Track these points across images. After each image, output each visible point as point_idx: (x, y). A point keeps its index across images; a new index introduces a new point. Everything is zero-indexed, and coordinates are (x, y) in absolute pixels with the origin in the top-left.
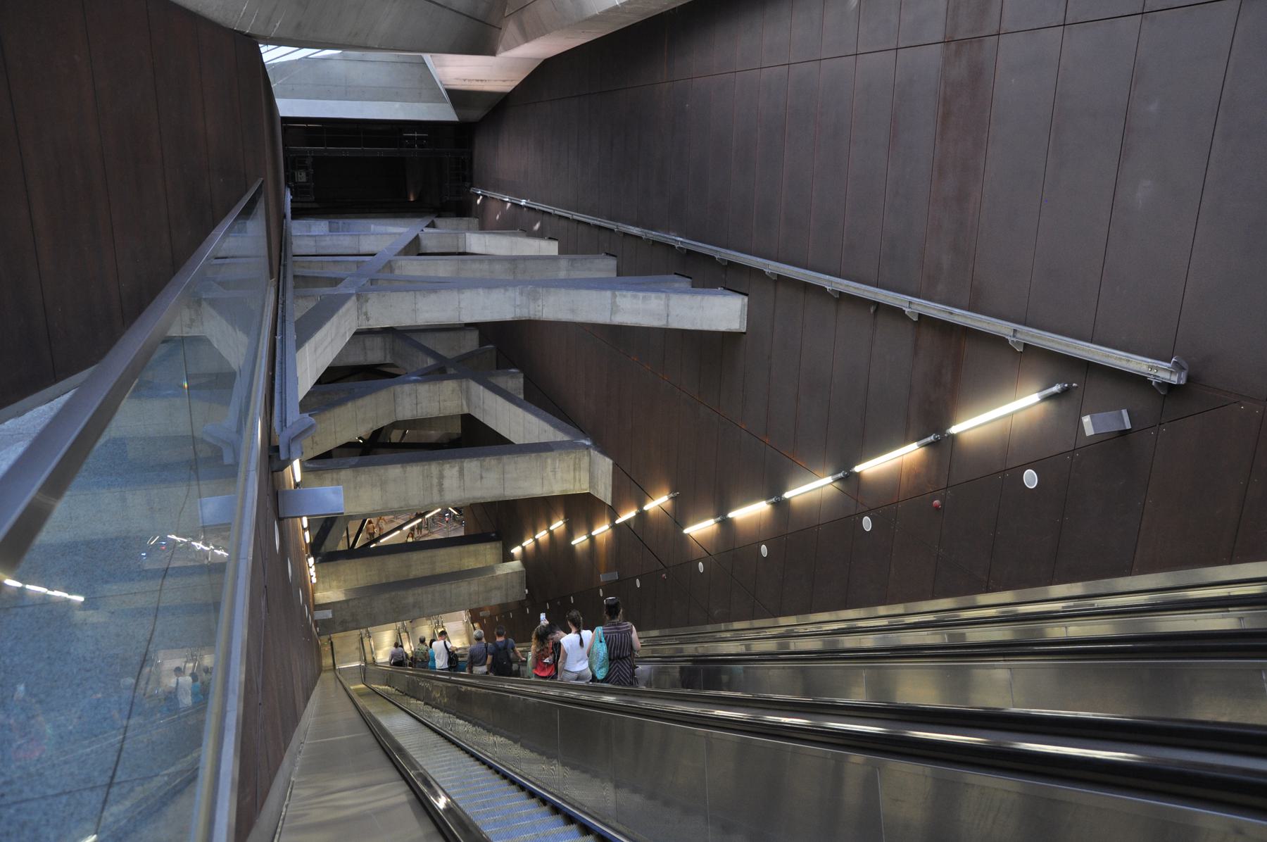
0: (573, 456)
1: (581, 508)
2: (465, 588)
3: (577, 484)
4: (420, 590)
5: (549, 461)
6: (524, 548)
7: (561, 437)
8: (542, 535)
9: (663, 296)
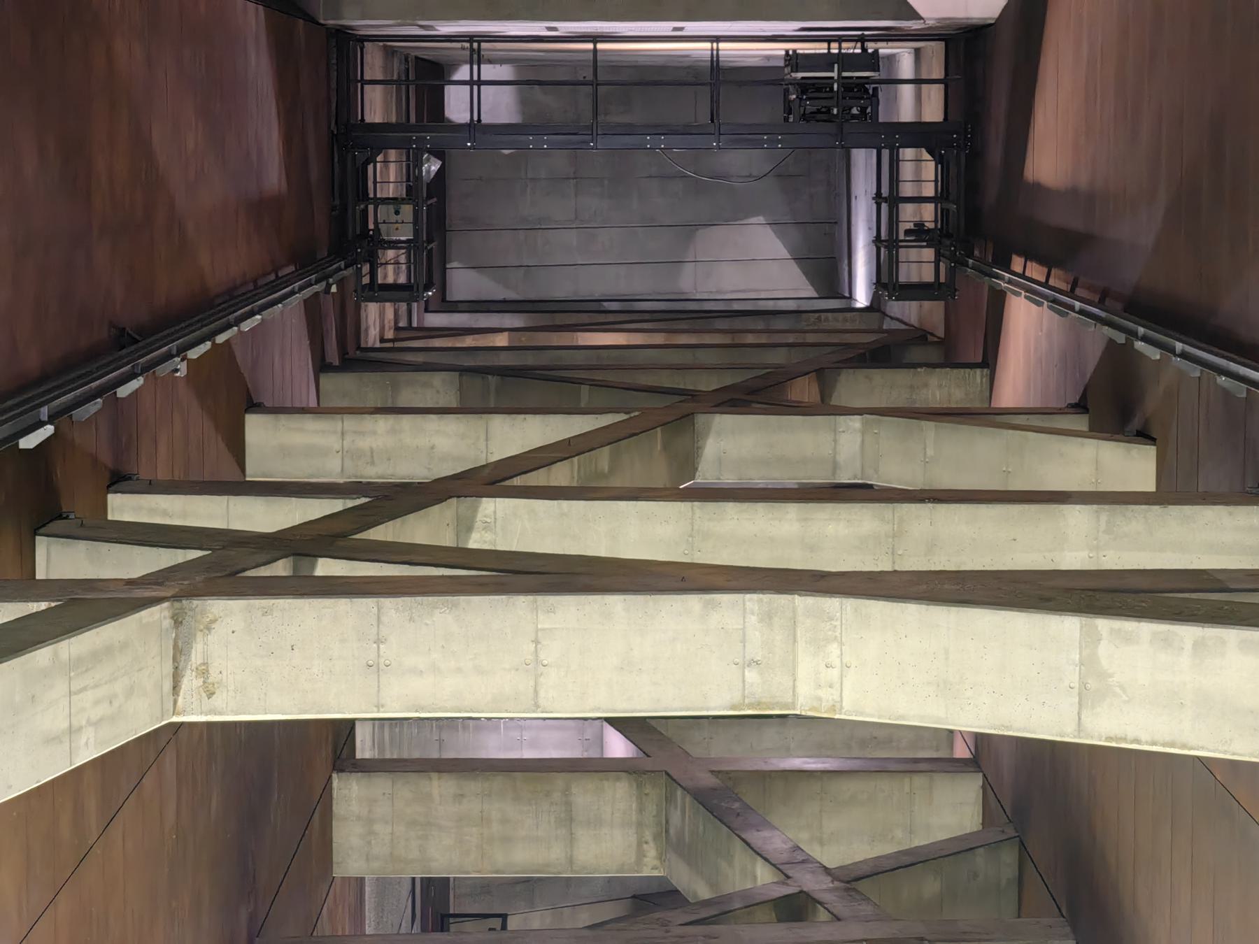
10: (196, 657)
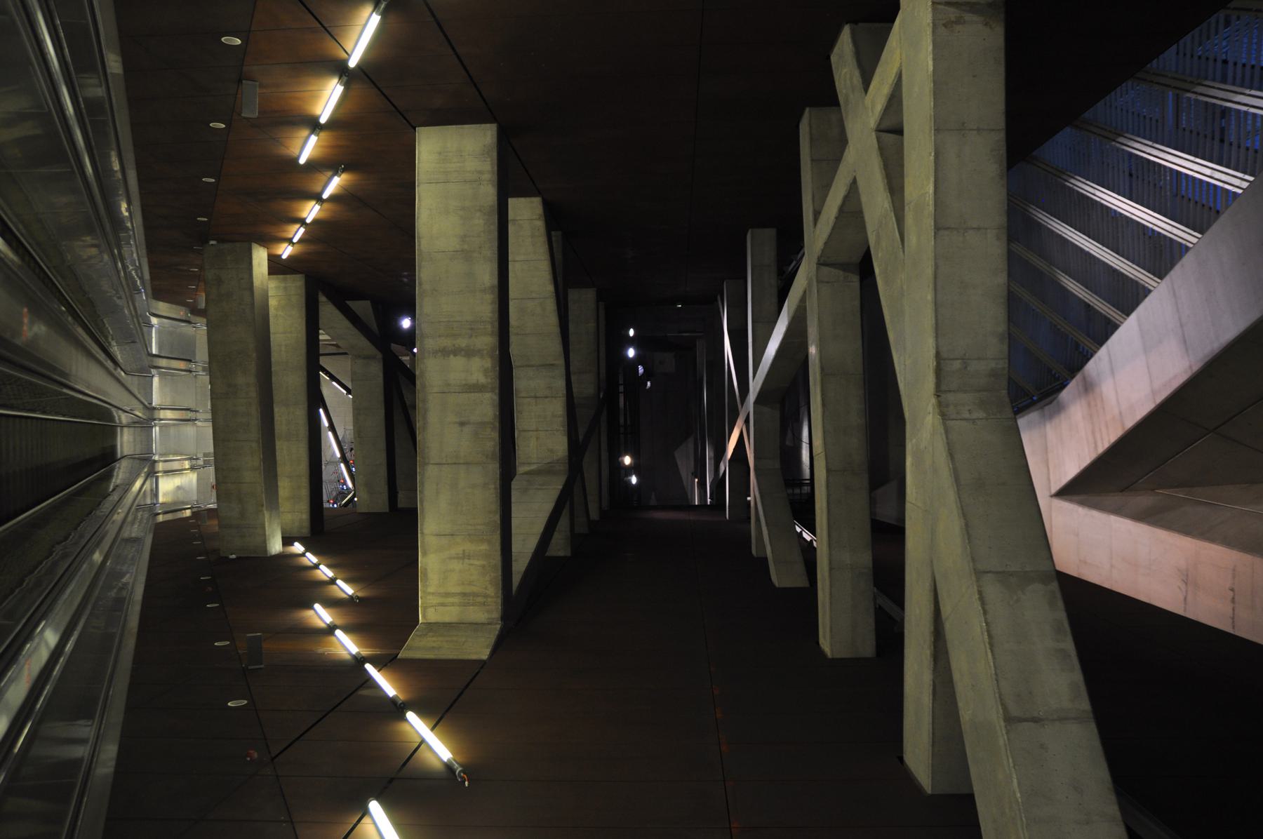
0: (491, 591)
2: (250, 462)
3: (434, 600)
4: (253, 394)
5: (484, 547)
7: (516, 580)
8: (325, 572)
9: (1085, 705)
10: (968, 17)
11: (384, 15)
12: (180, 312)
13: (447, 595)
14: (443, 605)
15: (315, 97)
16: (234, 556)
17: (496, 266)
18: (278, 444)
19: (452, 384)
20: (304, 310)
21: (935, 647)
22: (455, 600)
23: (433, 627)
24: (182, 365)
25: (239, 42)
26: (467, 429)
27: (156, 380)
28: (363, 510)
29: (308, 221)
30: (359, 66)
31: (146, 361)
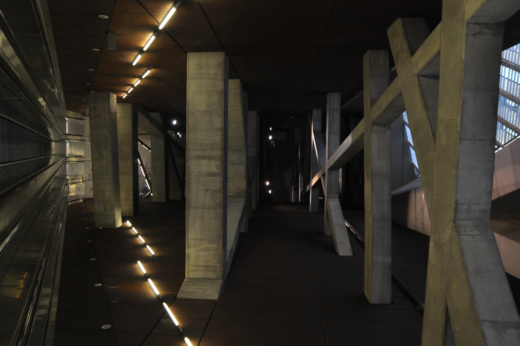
0: (218, 265)
1: (170, 269)
2: (108, 188)
5: (215, 246)
6: (131, 228)
8: (141, 240)
11: (178, 8)
12: (79, 115)
13: (198, 266)
14: (196, 270)
15: (142, 40)
16: (101, 228)
17: (223, 118)
18: (120, 176)
19: (202, 172)
20: (131, 119)
21: (444, 338)
22: (202, 268)
23: (192, 280)
24: (79, 138)
25: (107, 17)
26: (208, 193)
27: (68, 145)
28: (156, 201)
29: (135, 85)
30: (164, 29)
31: (63, 137)
